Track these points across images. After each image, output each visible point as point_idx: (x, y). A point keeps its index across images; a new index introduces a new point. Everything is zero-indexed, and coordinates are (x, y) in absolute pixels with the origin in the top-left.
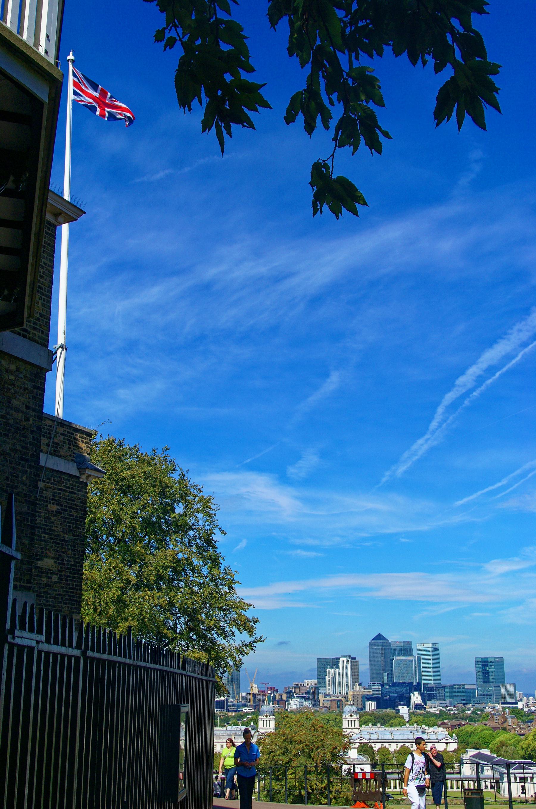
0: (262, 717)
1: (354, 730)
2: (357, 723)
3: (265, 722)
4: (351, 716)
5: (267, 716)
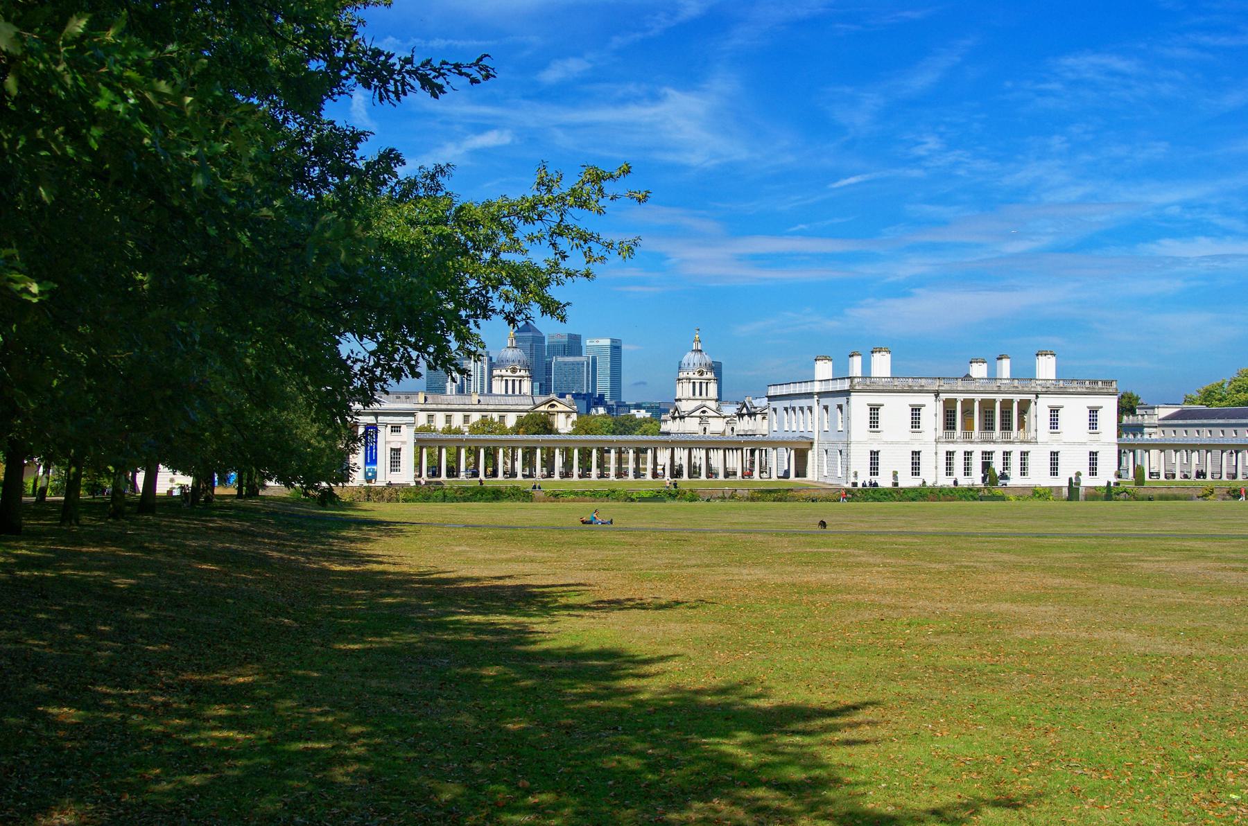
0: (503, 372)
1: (708, 403)
3: (510, 383)
4: (701, 373)
5: (514, 370)
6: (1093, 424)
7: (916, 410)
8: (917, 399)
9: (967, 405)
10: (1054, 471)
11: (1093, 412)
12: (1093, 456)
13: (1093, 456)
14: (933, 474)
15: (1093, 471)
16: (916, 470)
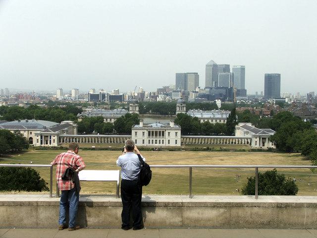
2: (185, 108)
4: (181, 104)
6: (176, 135)
7: (143, 133)
8: (144, 131)
9: (153, 132)
10: (169, 143)
11: (176, 133)
12: (176, 140)
13: (176, 140)
14: (146, 144)
15: (176, 143)
16: (143, 143)
